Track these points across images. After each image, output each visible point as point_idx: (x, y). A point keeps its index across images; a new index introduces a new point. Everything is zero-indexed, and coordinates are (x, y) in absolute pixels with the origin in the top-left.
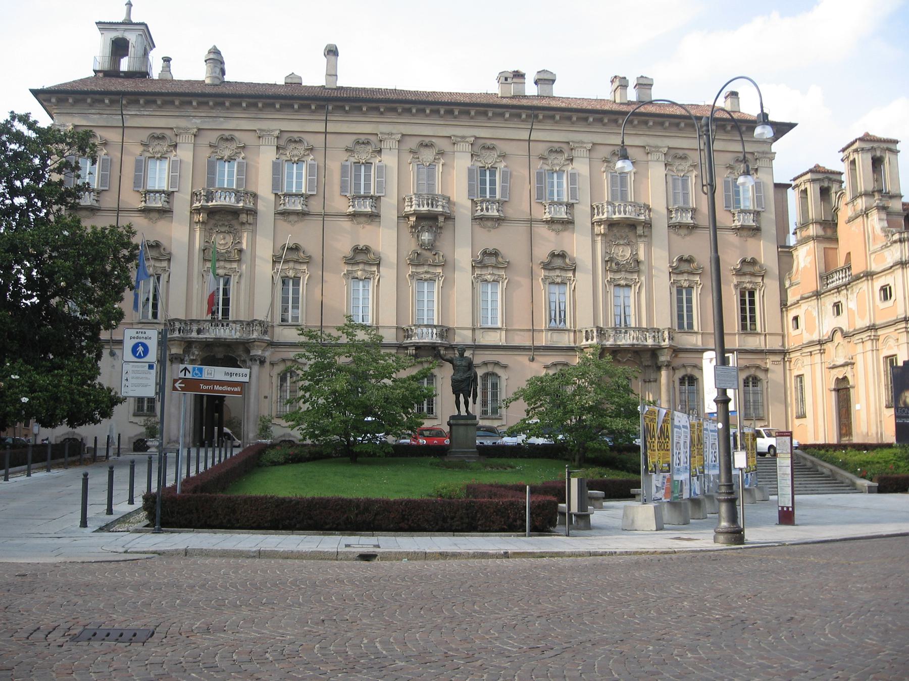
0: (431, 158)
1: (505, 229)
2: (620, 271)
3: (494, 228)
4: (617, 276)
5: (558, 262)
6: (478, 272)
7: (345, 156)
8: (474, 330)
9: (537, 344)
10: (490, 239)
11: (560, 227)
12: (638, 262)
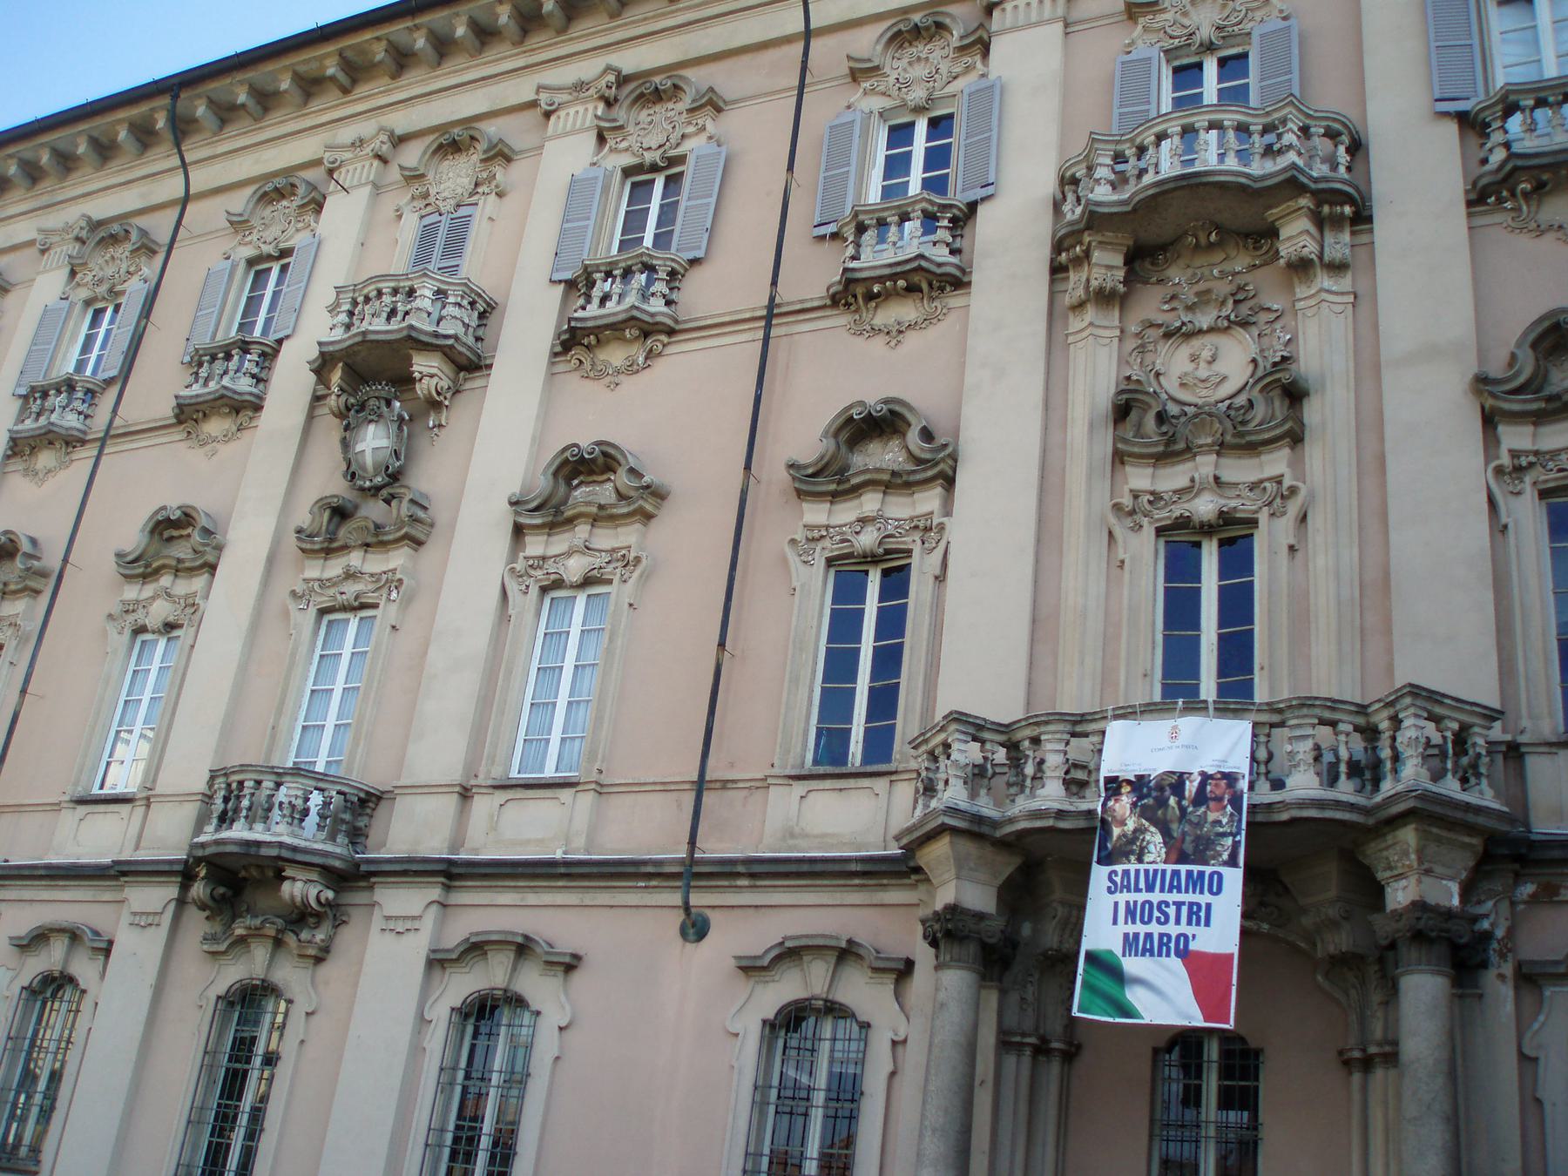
0: (466, 182)
1: (681, 364)
2: (1189, 452)
3: (631, 369)
4: (1173, 478)
5: (885, 455)
6: (535, 545)
7: (227, 243)
8: (465, 794)
9: (714, 847)
10: (597, 412)
11: (904, 311)
12: (1295, 394)
